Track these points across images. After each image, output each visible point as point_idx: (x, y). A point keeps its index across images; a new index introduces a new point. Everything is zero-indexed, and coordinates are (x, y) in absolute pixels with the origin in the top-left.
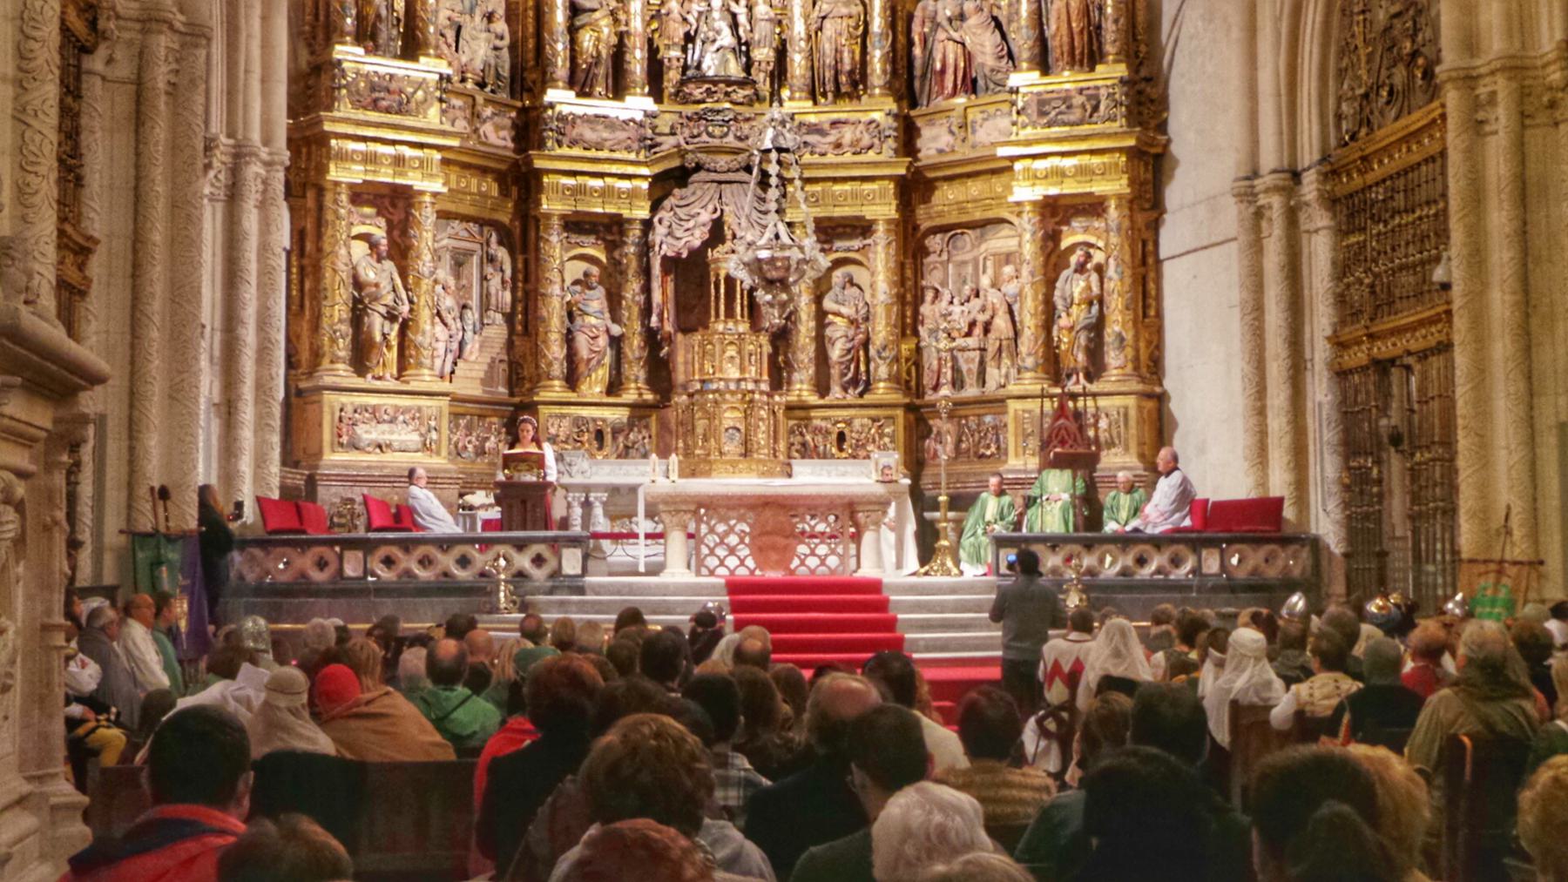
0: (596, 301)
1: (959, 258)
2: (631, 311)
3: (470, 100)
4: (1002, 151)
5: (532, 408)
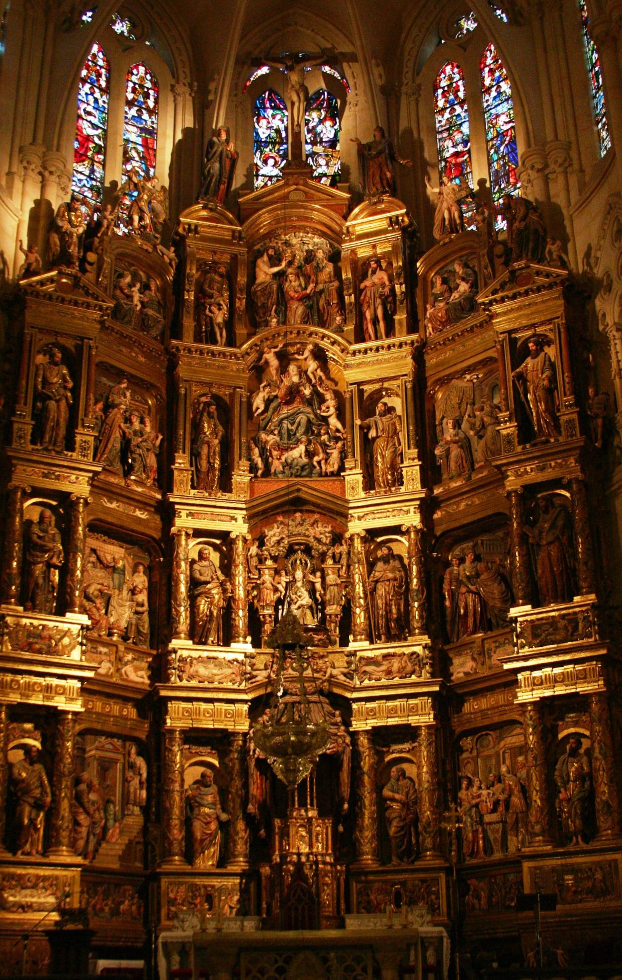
0: (210, 795)
1: (485, 753)
2: (235, 803)
3: (114, 649)
4: (507, 666)
5: (156, 877)
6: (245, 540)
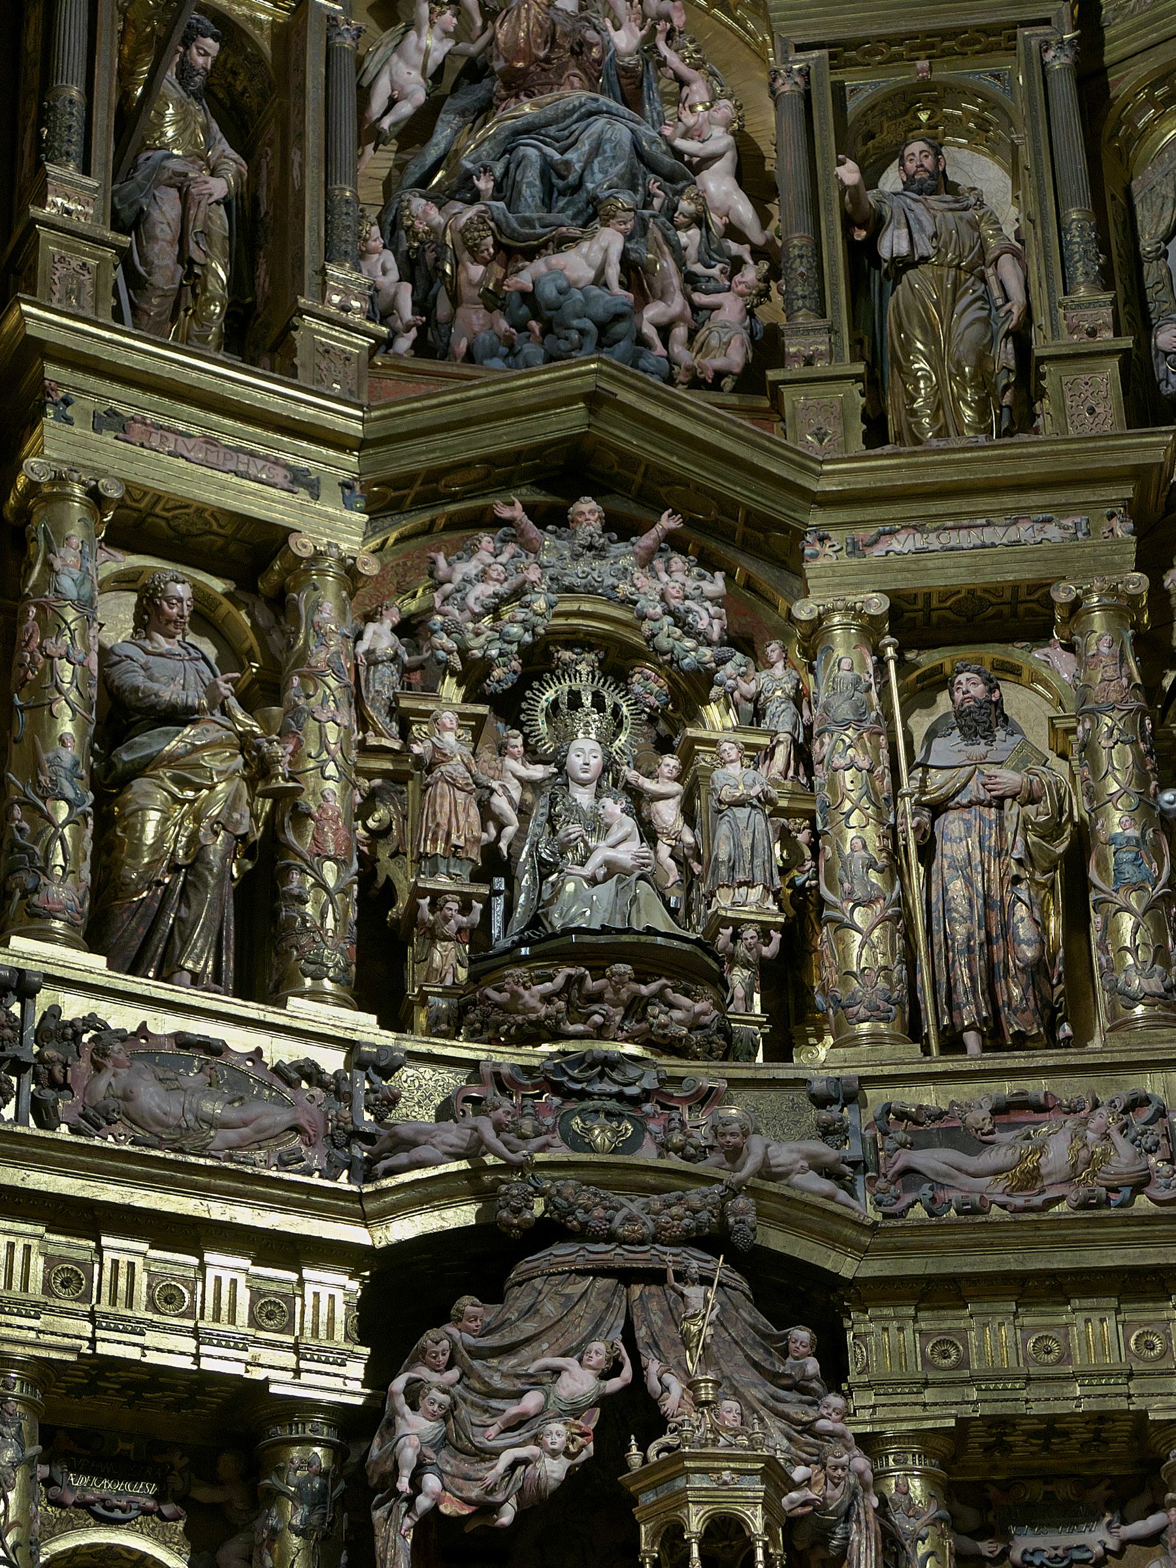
6: (350, 574)
